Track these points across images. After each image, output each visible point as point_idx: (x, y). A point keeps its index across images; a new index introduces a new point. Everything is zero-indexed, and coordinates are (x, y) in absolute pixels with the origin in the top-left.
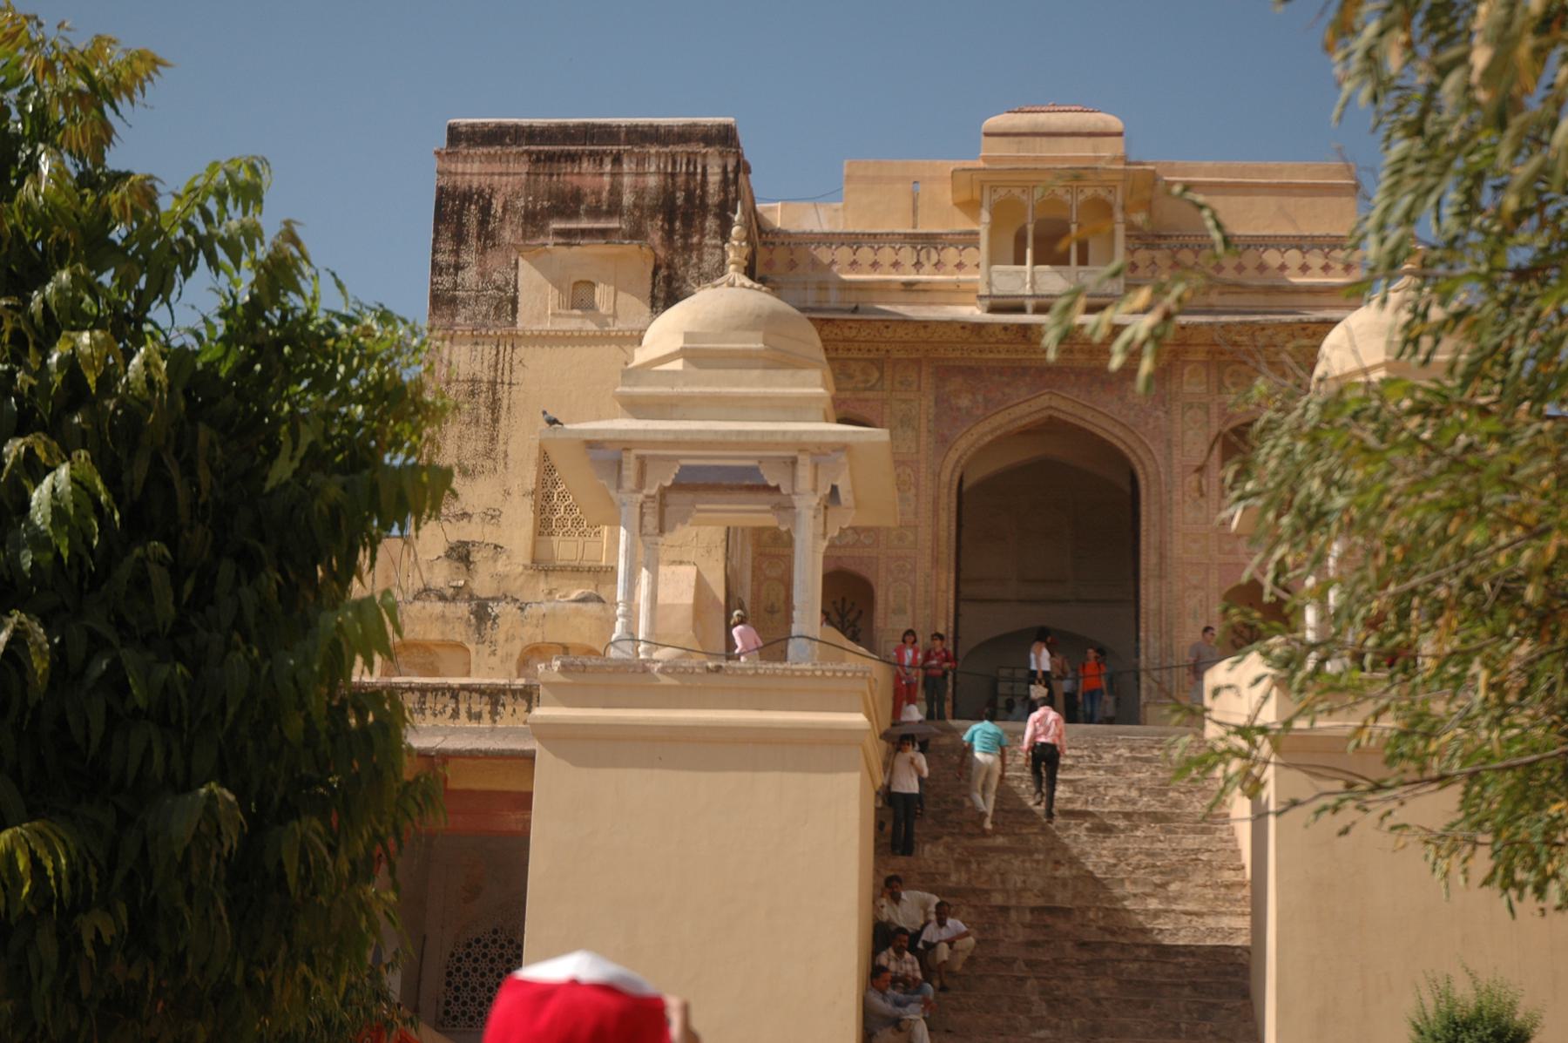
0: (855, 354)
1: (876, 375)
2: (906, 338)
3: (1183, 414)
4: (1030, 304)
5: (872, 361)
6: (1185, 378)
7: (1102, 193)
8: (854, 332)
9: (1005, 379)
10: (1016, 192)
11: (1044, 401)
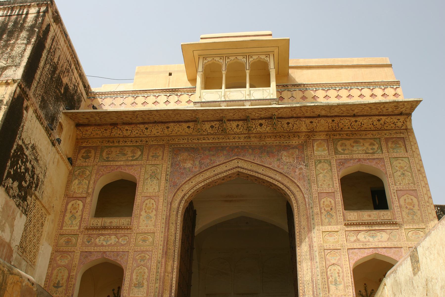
1: (139, 153)
2: (157, 134)
5: (137, 147)
6: (315, 148)
7: (263, 57)
8: (129, 132)
9: (211, 153)
11: (234, 164)
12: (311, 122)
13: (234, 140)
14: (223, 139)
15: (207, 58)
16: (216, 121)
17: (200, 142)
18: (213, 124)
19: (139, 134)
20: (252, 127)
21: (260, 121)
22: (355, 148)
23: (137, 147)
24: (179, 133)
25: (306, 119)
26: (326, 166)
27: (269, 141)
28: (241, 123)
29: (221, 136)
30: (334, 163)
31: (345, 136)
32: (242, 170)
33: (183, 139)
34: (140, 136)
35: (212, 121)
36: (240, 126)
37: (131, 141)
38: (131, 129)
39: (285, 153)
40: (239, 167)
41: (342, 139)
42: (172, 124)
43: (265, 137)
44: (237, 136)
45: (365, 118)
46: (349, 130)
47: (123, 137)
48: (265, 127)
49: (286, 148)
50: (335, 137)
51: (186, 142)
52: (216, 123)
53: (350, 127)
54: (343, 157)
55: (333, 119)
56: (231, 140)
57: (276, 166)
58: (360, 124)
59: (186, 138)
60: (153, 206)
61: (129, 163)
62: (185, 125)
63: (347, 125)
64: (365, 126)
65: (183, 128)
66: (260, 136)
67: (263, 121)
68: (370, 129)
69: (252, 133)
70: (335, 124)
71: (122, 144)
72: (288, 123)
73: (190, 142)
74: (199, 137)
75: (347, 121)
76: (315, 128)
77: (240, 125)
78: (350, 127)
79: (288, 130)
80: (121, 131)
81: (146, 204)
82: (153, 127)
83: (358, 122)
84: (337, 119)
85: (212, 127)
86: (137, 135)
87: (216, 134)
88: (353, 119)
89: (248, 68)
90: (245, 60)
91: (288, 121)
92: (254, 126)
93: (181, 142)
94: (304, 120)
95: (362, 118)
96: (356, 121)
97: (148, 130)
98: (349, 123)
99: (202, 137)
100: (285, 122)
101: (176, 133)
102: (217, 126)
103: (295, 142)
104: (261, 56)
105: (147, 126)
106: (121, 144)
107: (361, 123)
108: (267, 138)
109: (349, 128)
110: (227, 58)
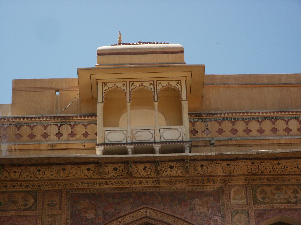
0: (18, 189)
1: (32, 201)
2: (51, 177)
3: (232, 217)
4: (130, 148)
5: (29, 192)
6: (232, 196)
7: (173, 83)
8: (17, 175)
9: (115, 200)
10: (119, 85)
11: (142, 213)
12: (228, 165)
13: (140, 186)
14: (129, 183)
15: (108, 84)
16: (120, 163)
17: (102, 187)
18: (117, 166)
19: (29, 177)
20: (161, 170)
21: (171, 164)
22: (276, 197)
24: (77, 176)
25: (223, 162)
26: (244, 217)
27: (180, 186)
28: (148, 165)
29: (126, 180)
30: (252, 214)
31: (266, 181)
32: (150, 221)
33: (83, 184)
34: (32, 179)
35: (116, 163)
36: (147, 169)
37: (21, 186)
38: (20, 171)
39: (198, 201)
40: (147, 217)
41: (262, 185)
42: (69, 166)
43: (176, 181)
44: (144, 180)
45: (289, 161)
46: (270, 173)
47: (11, 181)
48: (176, 170)
49: (200, 195)
50: (255, 183)
51: (86, 187)
52: (119, 165)
53: (272, 170)
54: (263, 207)
55: (253, 161)
56: (138, 186)
57: (189, 217)
58: (283, 167)
59: (85, 181)
61: (22, 214)
62: (84, 167)
63: (268, 168)
64: (289, 169)
65: (81, 170)
66: (171, 181)
68: (294, 173)
69: (161, 177)
70: (255, 167)
71: (10, 189)
72: (202, 166)
73: (91, 187)
74: (101, 181)
75: (268, 164)
76: (232, 171)
77: (148, 167)
78: (272, 170)
79: (202, 173)
80: (7, 173)
82: (46, 169)
83: (281, 165)
84: (257, 162)
85: (115, 169)
86: (27, 178)
87: (120, 178)
88: (275, 162)
89: (156, 100)
90: (152, 87)
91: (202, 163)
92: (163, 169)
93: (80, 187)
94: (220, 162)
95: (286, 161)
96: (279, 164)
97: (41, 172)
98: (271, 166)
99: (104, 180)
100: (199, 164)
101: (74, 176)
102: (121, 168)
103: (209, 188)
104: (171, 83)
105: (39, 168)
106: (8, 190)
107: (285, 166)
108: (178, 182)
109: (270, 172)
110: (131, 84)
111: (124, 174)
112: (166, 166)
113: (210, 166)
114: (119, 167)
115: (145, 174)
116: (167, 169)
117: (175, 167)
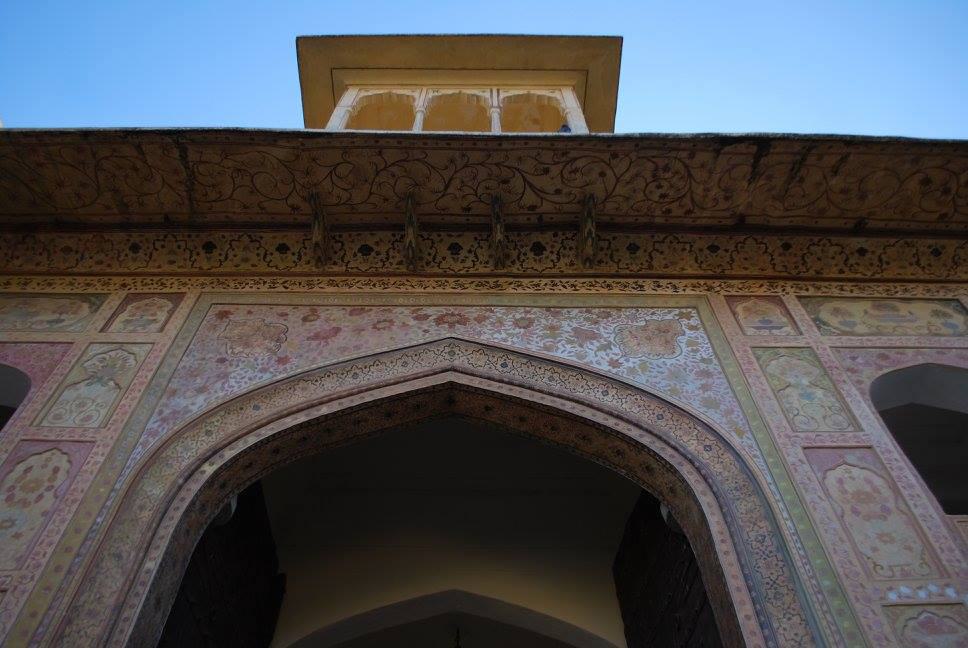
23: (84, 297)
28: (467, 241)
36: (463, 253)
40: (454, 370)
44: (451, 280)
45: (892, 241)
48: (554, 257)
52: (380, 234)
55: (786, 238)
60: (52, 479)
65: (262, 253)
67: (546, 238)
77: (466, 248)
80: (45, 255)
81: (28, 470)
82: (158, 244)
83: (868, 255)
91: (633, 238)
92: (514, 254)
94: (690, 237)
102: (383, 248)
105: (135, 238)
111: (391, 264)
112: (522, 247)
113: (657, 251)
114: (377, 243)
115: (457, 266)
116: (525, 254)
117: (549, 249)
